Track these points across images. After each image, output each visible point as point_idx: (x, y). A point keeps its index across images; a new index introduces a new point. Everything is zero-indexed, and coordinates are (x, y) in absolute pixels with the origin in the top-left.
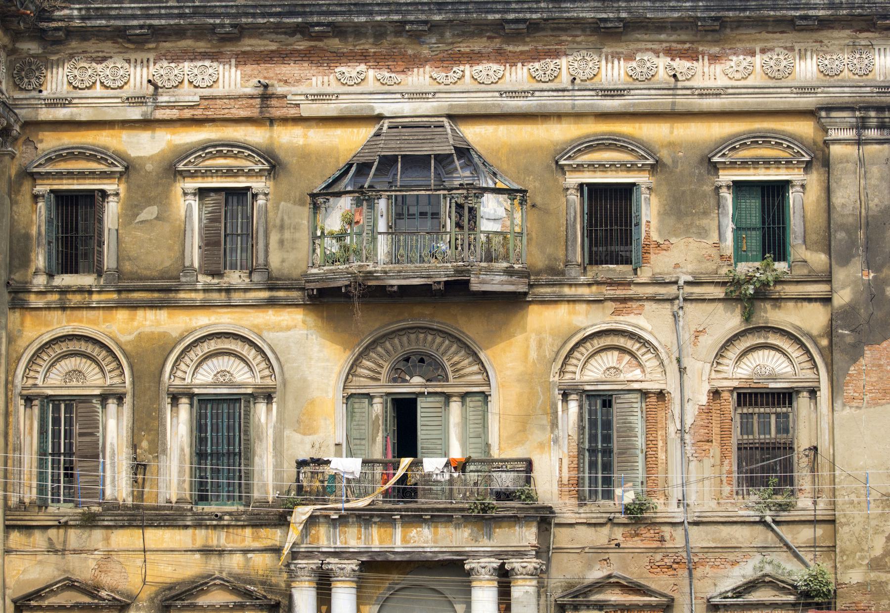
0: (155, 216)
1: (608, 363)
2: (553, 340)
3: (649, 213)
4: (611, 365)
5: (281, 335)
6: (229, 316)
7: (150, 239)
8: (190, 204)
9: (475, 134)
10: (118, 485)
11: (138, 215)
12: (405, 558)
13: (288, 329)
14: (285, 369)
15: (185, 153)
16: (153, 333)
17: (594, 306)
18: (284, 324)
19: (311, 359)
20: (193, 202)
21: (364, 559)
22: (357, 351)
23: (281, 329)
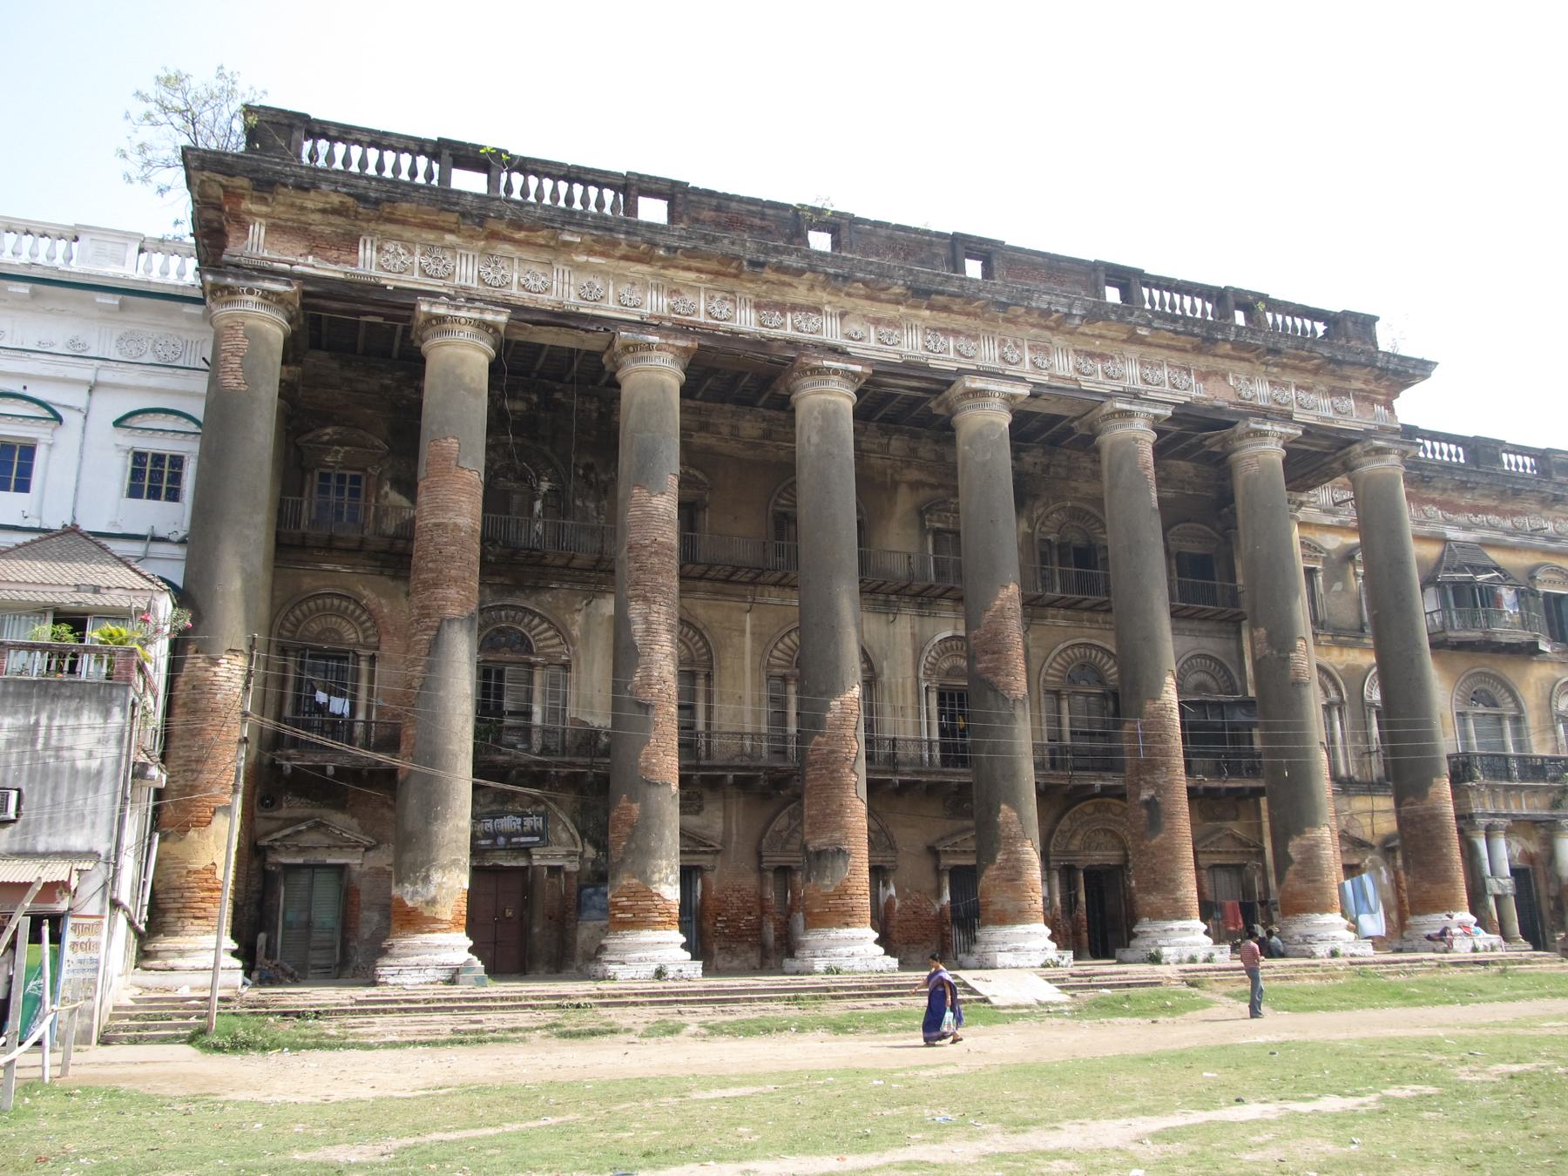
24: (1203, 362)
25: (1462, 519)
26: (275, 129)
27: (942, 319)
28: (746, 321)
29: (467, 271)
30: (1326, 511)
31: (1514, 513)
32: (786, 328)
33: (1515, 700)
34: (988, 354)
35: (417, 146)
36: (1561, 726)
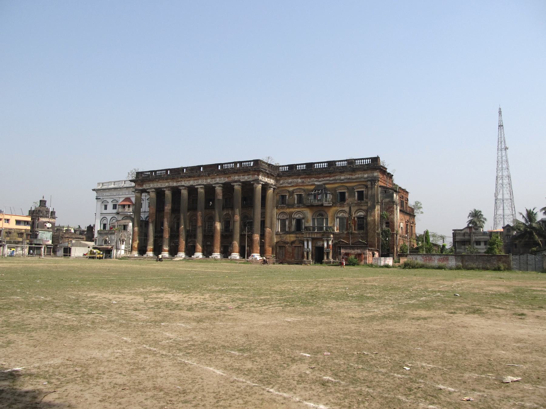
3: (347, 195)
9: (327, 186)
10: (287, 230)
15: (294, 190)
24: (228, 175)
25: (320, 180)
26: (138, 174)
27: (194, 178)
28: (175, 184)
29: (152, 185)
30: (289, 184)
31: (334, 176)
32: (179, 184)
34: (200, 182)
35: (149, 172)
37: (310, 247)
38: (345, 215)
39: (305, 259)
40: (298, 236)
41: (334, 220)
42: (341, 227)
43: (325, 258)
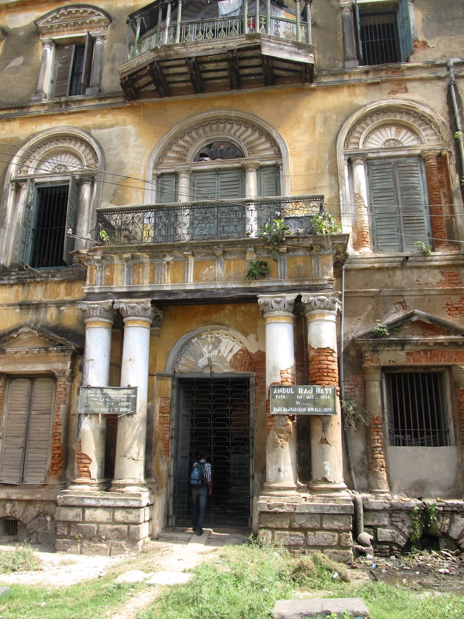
0: (21, 63)
1: (387, 136)
2: (337, 116)
4: (390, 138)
5: (105, 131)
6: (66, 121)
7: (15, 78)
8: (46, 50)
11: (9, 63)
12: (197, 296)
13: (112, 126)
14: (106, 155)
16: (6, 139)
17: (372, 88)
18: (108, 123)
19: (128, 146)
20: (48, 50)
21: (156, 298)
22: (166, 139)
23: (105, 127)
33: (274, 144)
36: (360, 170)
37: (136, 372)
38: (407, 139)
39: (86, 487)
40: (37, 294)
41: (334, 172)
42: (390, 211)
43: (283, 464)
